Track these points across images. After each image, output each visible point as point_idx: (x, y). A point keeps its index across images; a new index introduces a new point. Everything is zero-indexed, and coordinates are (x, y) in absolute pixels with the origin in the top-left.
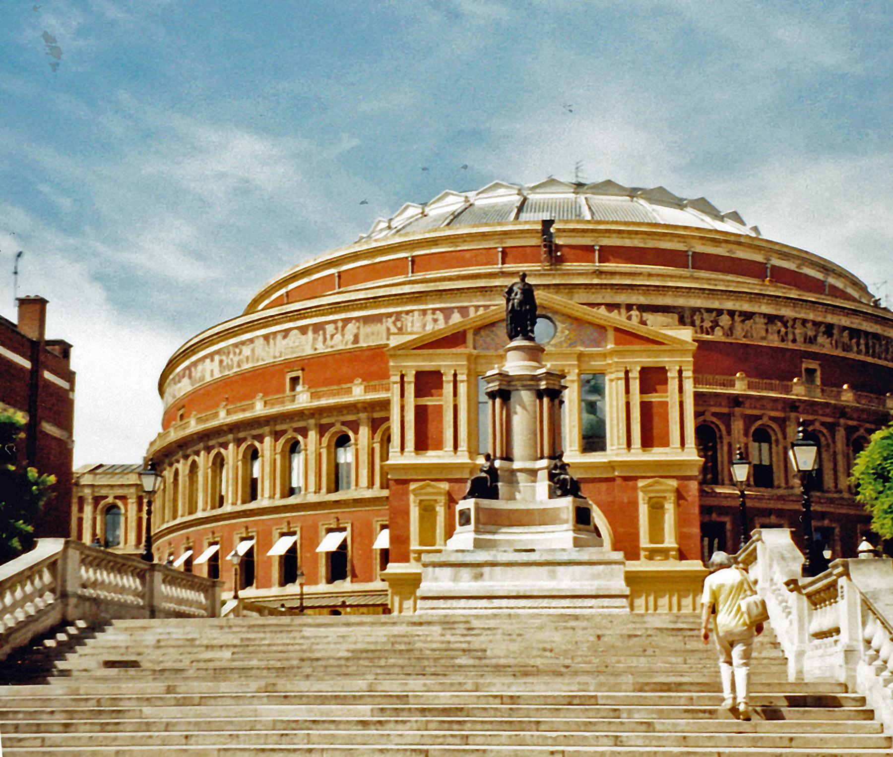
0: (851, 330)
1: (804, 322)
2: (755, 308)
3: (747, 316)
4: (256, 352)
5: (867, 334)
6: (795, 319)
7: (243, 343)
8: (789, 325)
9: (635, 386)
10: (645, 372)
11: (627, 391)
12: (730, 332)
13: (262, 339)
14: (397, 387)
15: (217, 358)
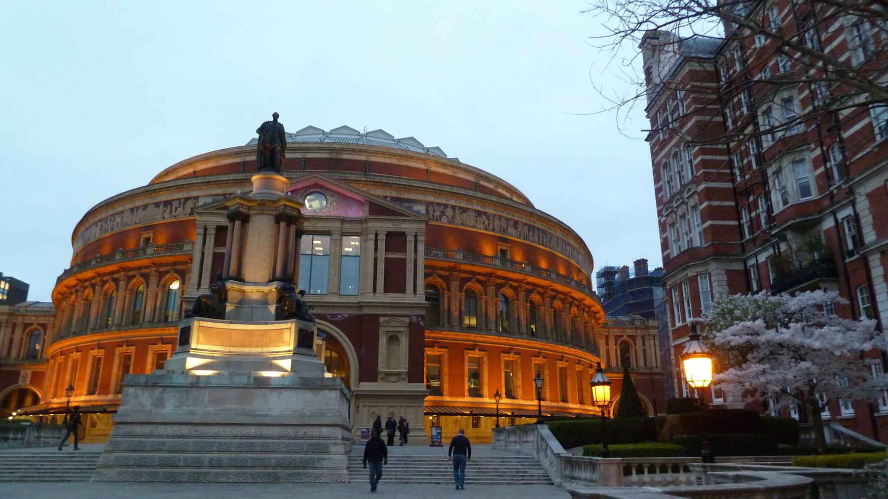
0: (529, 226)
1: (500, 217)
2: (470, 207)
3: (464, 210)
4: (125, 220)
5: (539, 229)
6: (494, 215)
7: (117, 214)
8: (491, 218)
9: (382, 245)
10: (389, 235)
11: (376, 250)
12: (452, 220)
13: (129, 212)
14: (199, 239)
15: (99, 224)
